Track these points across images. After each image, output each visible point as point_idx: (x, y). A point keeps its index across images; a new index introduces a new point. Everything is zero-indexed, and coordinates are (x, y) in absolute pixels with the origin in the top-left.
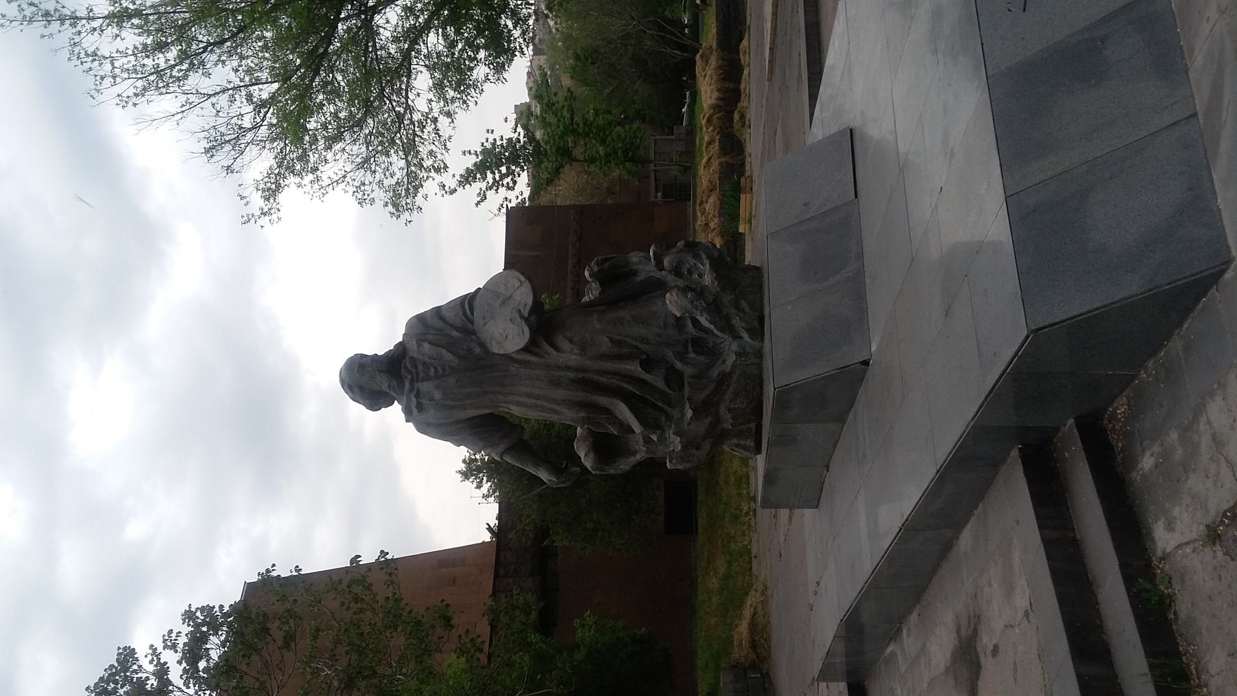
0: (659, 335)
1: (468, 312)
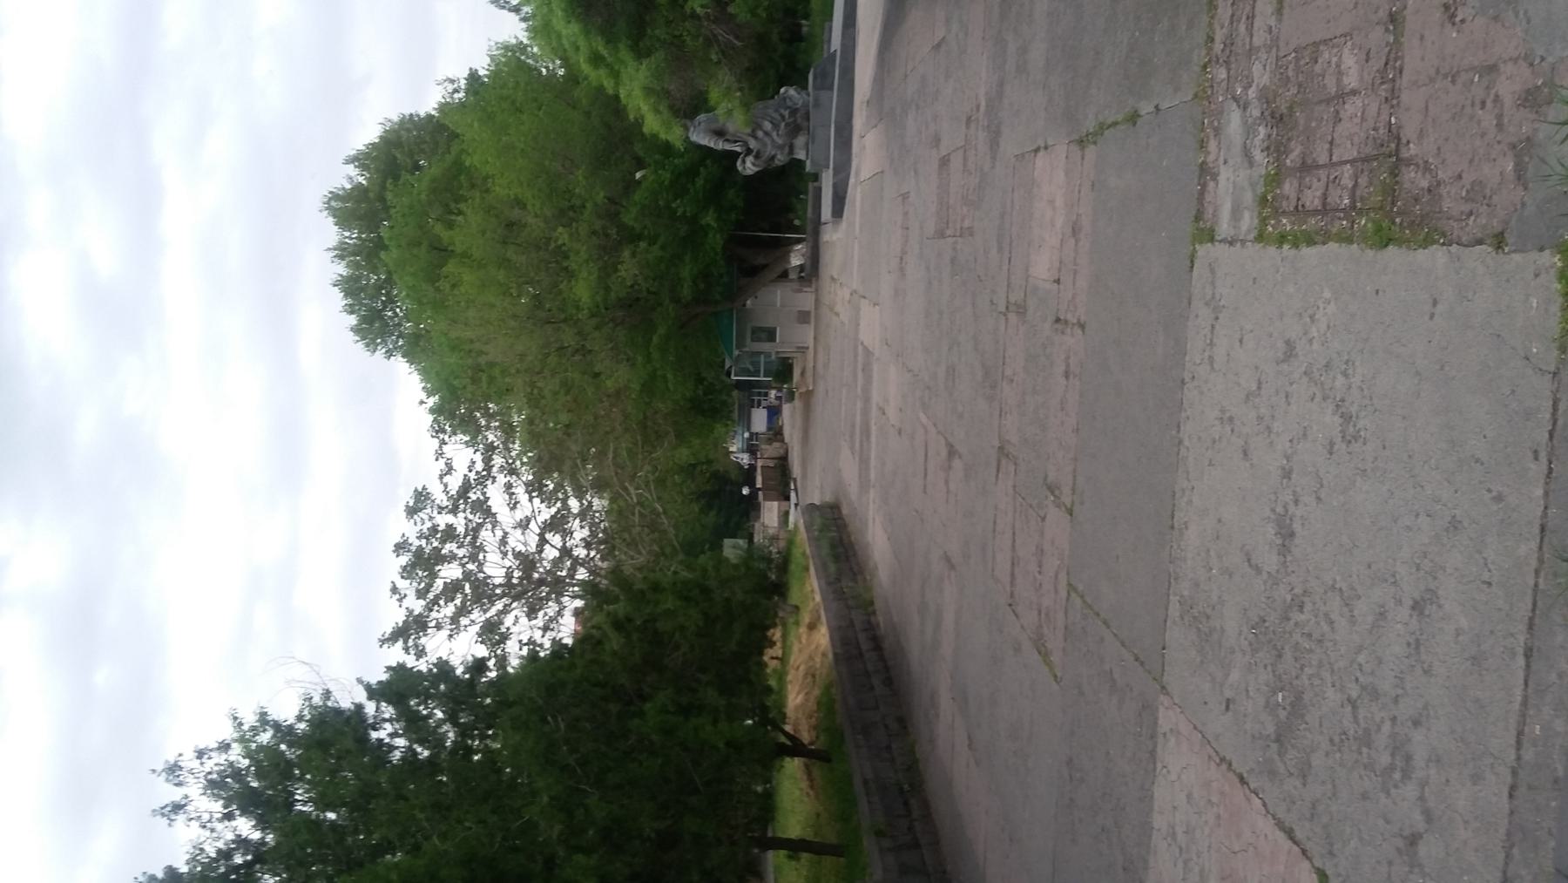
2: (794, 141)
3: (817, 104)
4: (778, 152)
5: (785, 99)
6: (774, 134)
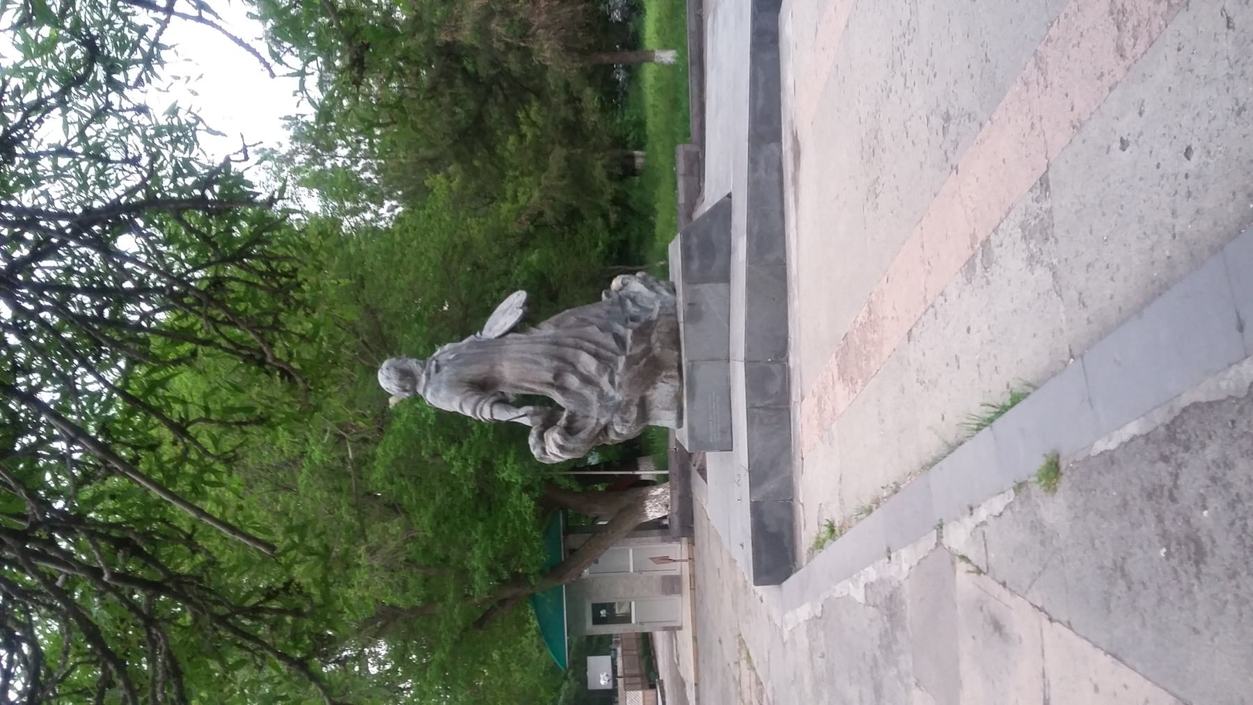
0: (609, 312)
2: (648, 393)
3: (694, 313)
4: (617, 419)
5: (621, 301)
6: (604, 381)
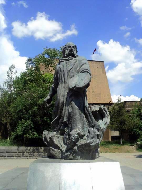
1: (83, 71)
